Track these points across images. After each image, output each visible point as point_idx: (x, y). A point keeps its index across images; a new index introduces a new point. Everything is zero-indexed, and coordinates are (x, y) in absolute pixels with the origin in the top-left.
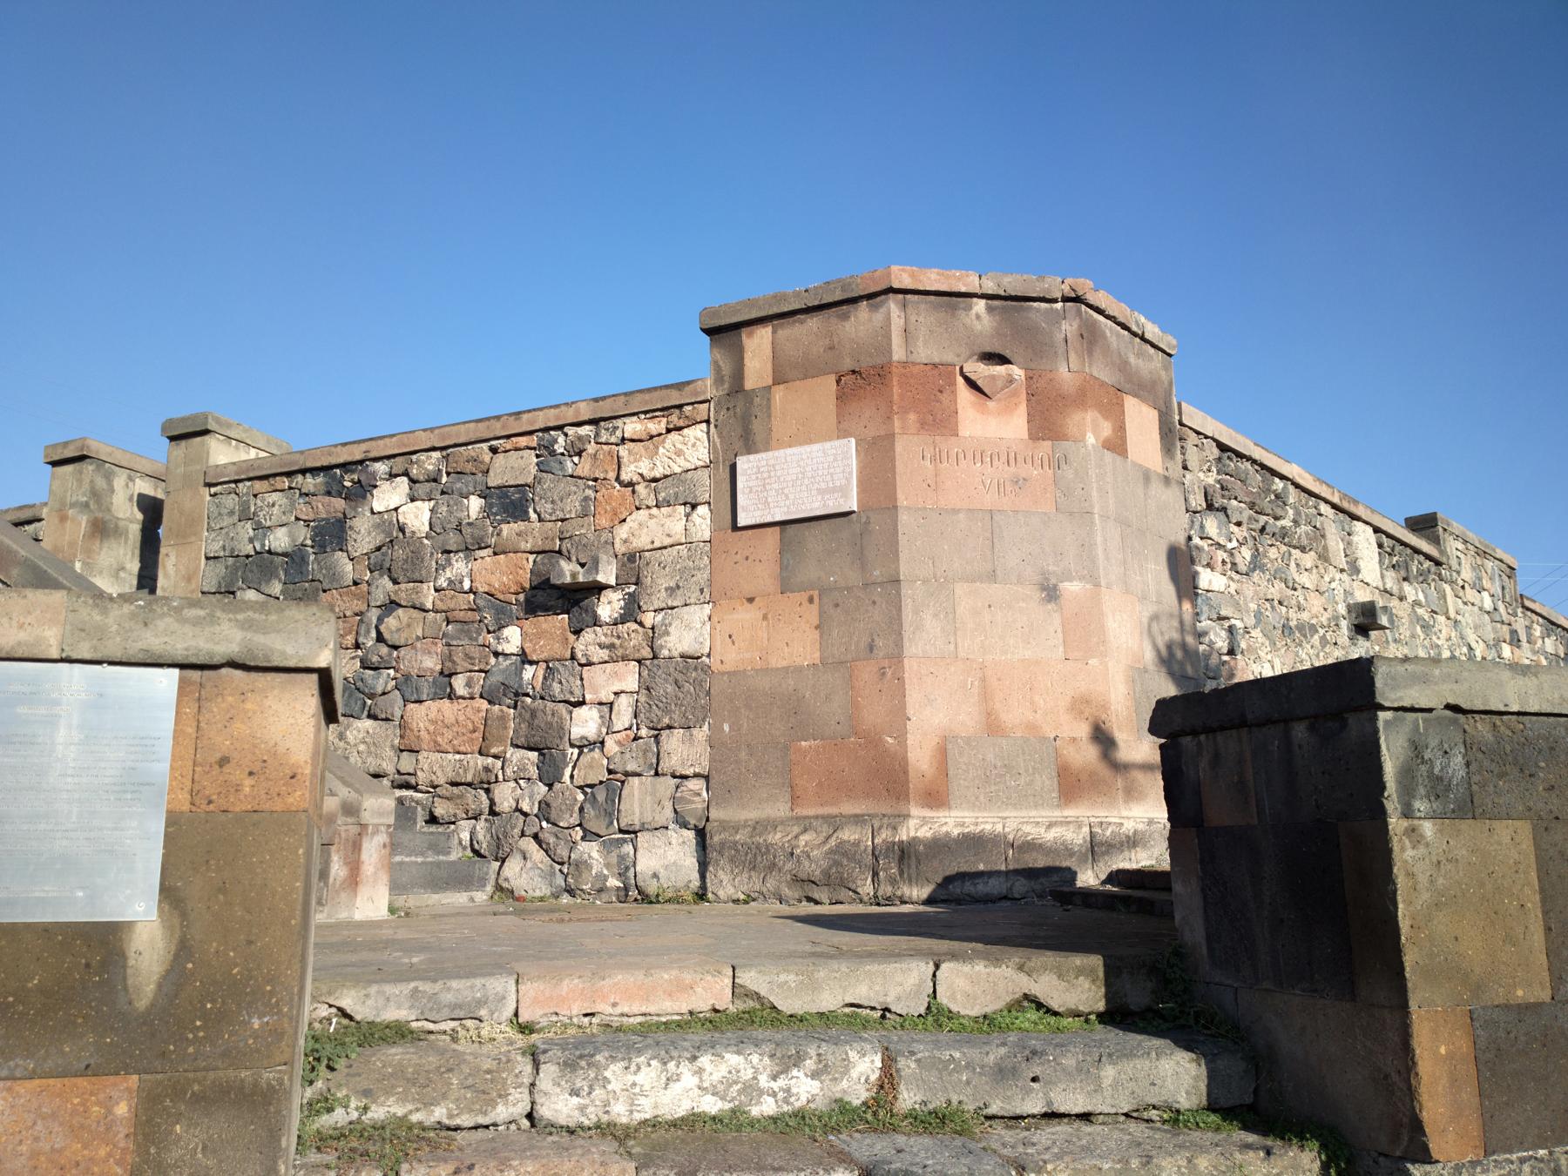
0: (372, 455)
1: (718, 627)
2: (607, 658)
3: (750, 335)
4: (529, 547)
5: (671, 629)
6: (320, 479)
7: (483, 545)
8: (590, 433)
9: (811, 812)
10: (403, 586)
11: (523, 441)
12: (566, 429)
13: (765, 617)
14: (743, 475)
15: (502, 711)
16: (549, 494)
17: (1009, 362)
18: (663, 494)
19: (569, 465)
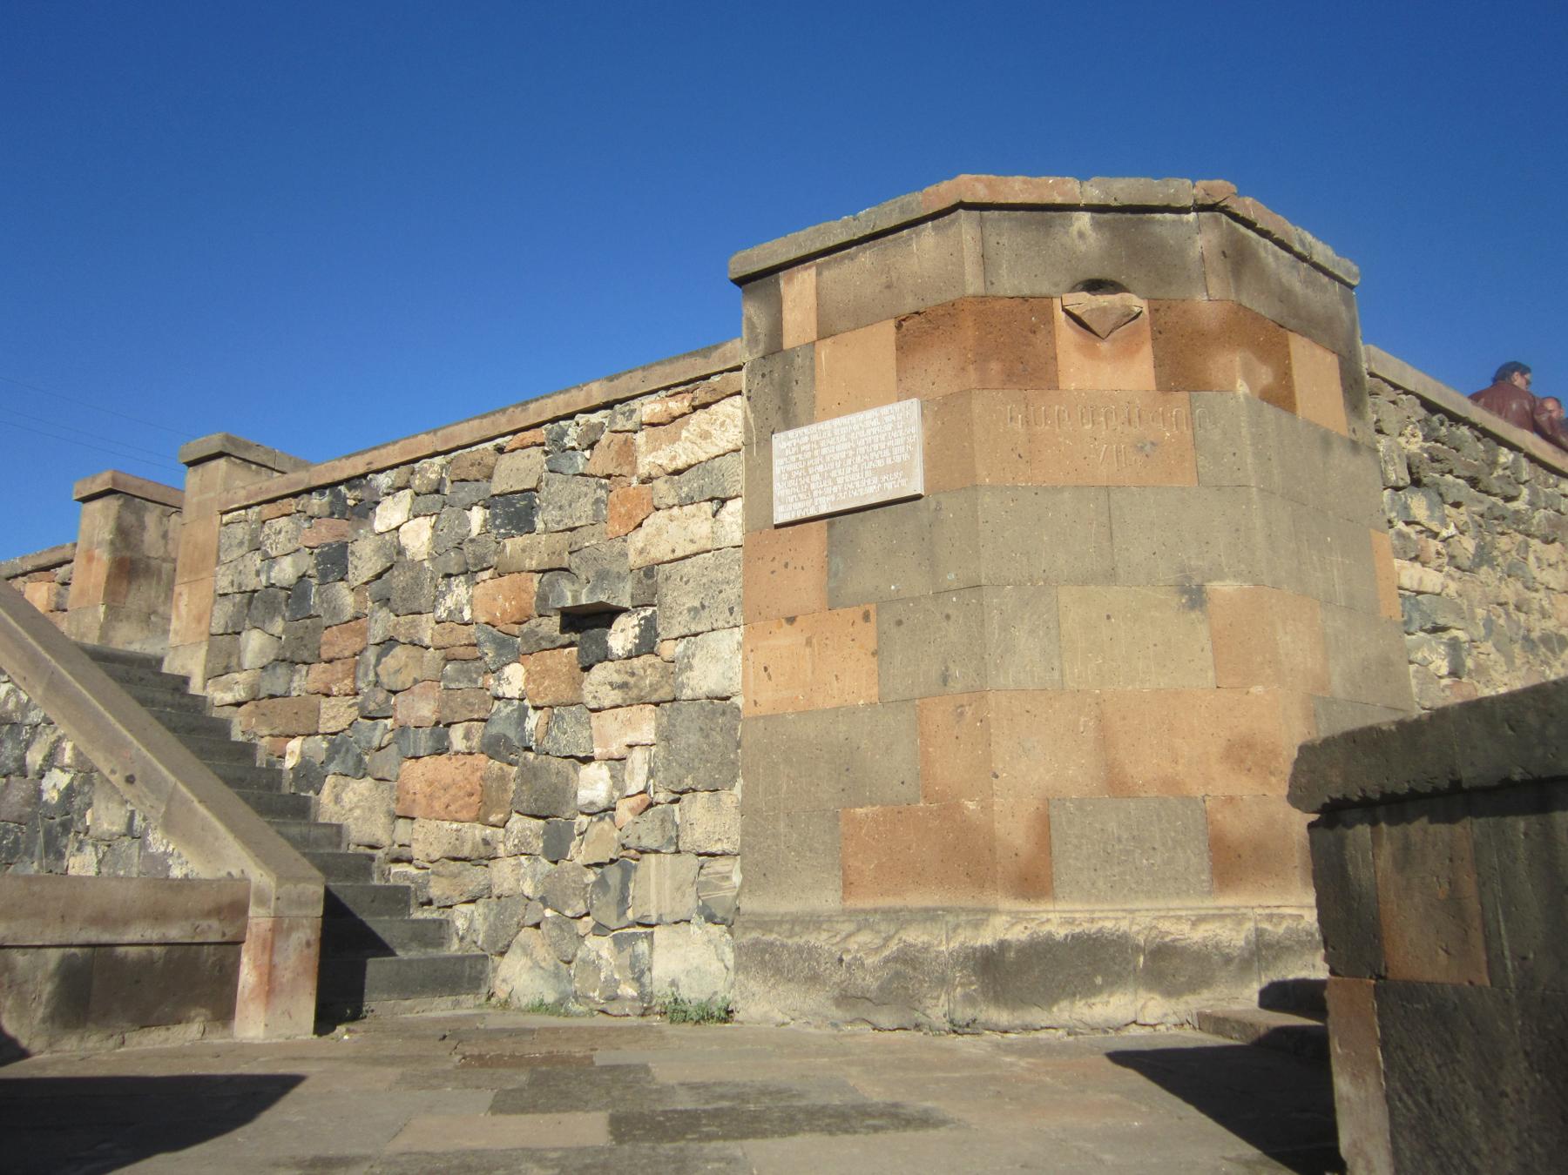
0: (375, 467)
1: (751, 656)
2: (619, 702)
3: (790, 280)
4: (534, 565)
5: (695, 662)
6: (326, 499)
7: (485, 565)
8: (604, 420)
9: (868, 904)
10: (402, 619)
11: (529, 436)
12: (578, 417)
13: (809, 643)
14: (780, 457)
15: (501, 769)
16: (557, 499)
17: (1129, 292)
18: (686, 489)
19: (580, 460)
